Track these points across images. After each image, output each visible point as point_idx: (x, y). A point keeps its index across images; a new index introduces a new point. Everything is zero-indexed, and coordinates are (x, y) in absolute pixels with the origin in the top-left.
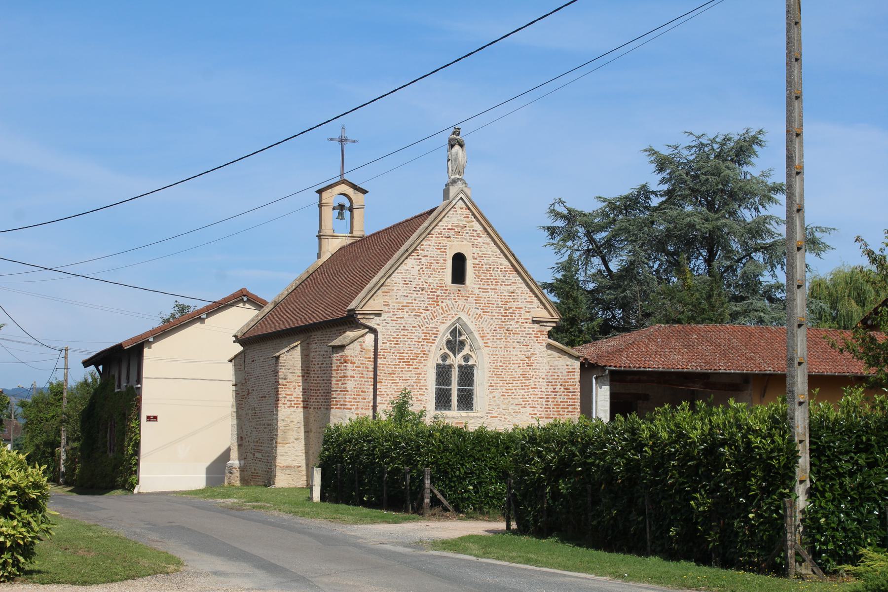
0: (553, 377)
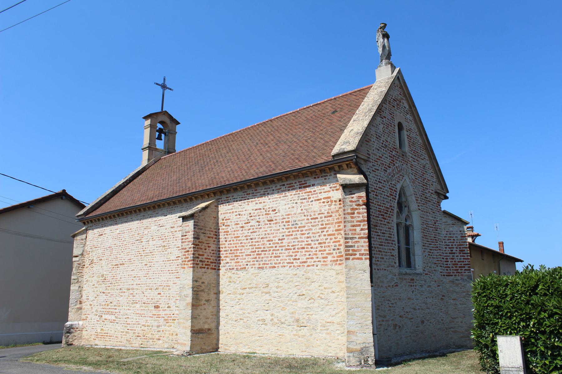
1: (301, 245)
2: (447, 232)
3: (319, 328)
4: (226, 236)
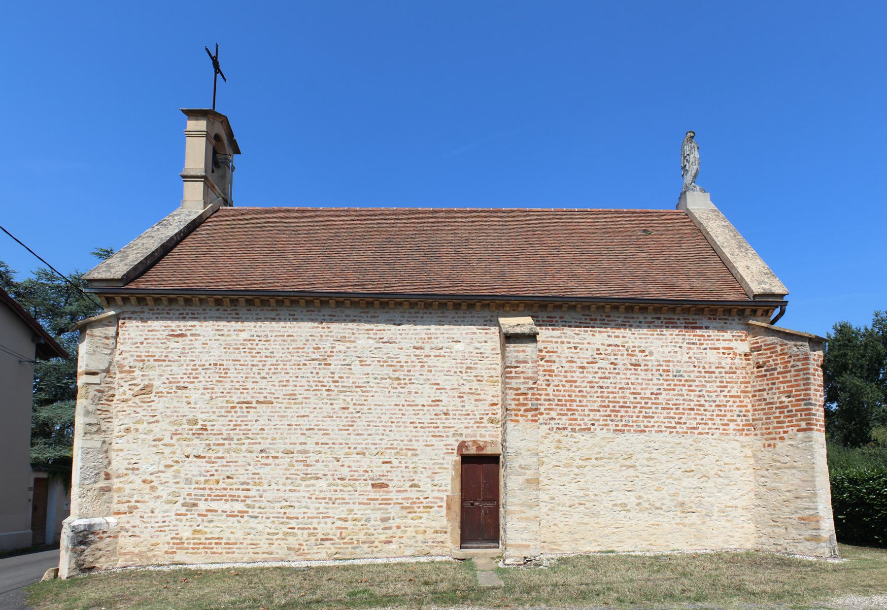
3: (716, 514)
4: (547, 377)
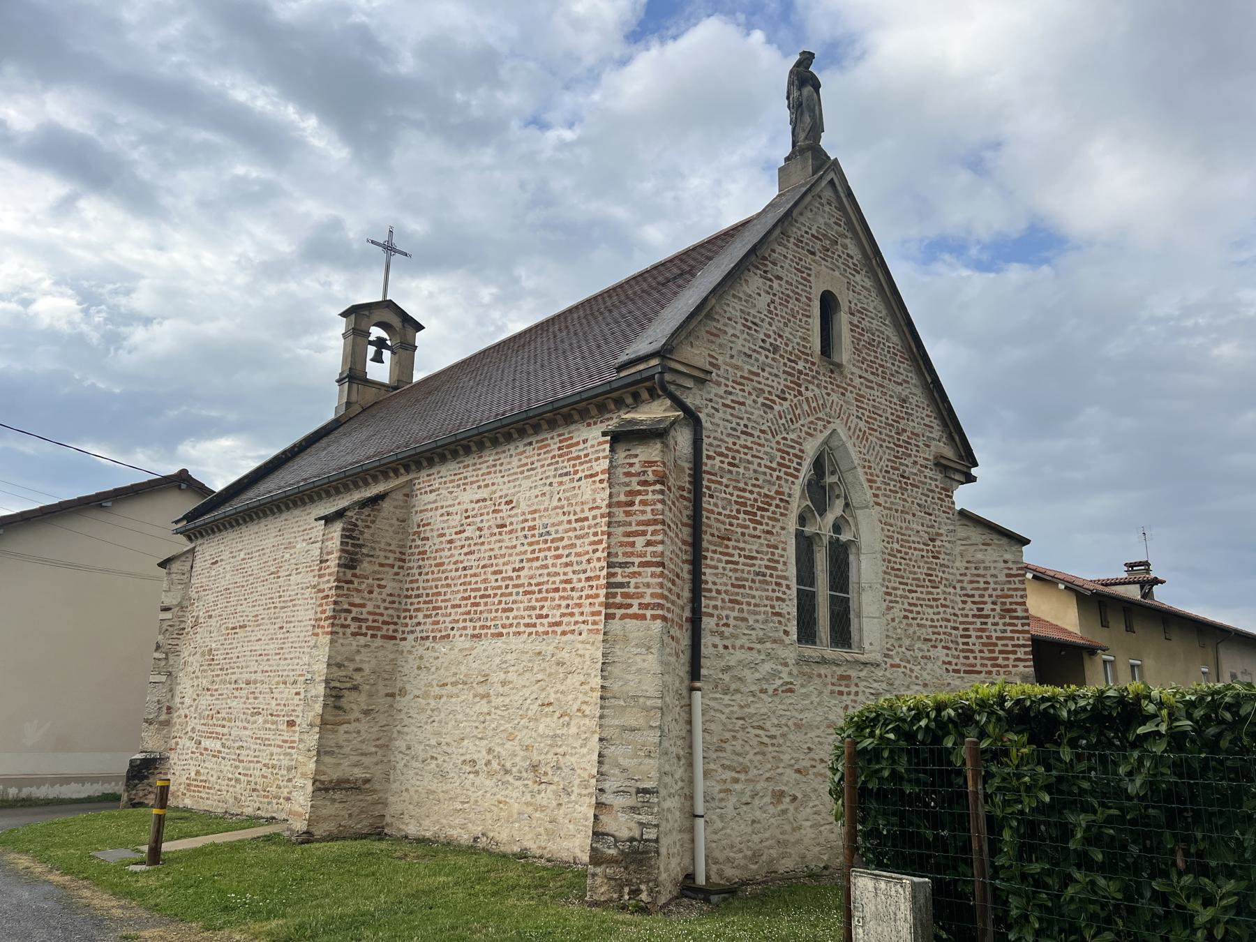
0: (975, 585)
1: (554, 582)
2: (968, 562)
4: (421, 563)
